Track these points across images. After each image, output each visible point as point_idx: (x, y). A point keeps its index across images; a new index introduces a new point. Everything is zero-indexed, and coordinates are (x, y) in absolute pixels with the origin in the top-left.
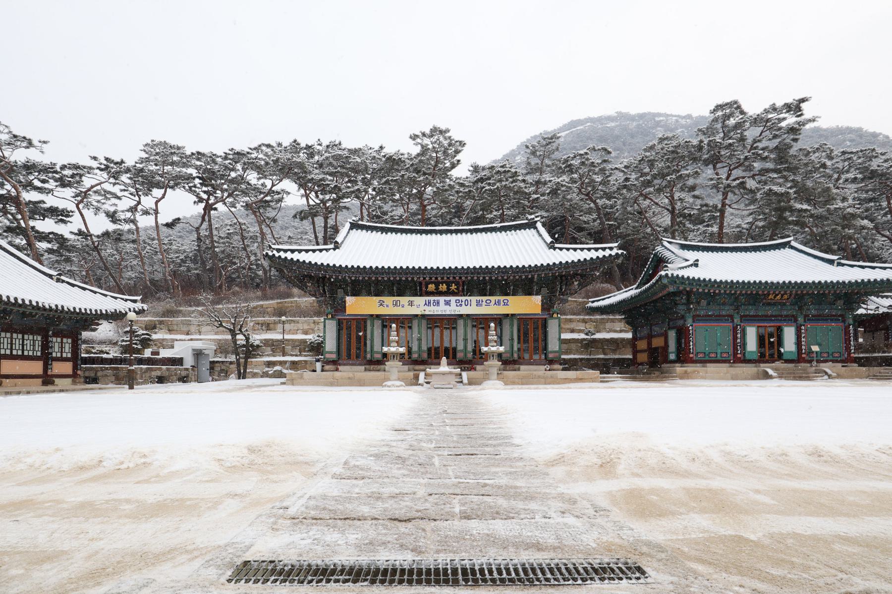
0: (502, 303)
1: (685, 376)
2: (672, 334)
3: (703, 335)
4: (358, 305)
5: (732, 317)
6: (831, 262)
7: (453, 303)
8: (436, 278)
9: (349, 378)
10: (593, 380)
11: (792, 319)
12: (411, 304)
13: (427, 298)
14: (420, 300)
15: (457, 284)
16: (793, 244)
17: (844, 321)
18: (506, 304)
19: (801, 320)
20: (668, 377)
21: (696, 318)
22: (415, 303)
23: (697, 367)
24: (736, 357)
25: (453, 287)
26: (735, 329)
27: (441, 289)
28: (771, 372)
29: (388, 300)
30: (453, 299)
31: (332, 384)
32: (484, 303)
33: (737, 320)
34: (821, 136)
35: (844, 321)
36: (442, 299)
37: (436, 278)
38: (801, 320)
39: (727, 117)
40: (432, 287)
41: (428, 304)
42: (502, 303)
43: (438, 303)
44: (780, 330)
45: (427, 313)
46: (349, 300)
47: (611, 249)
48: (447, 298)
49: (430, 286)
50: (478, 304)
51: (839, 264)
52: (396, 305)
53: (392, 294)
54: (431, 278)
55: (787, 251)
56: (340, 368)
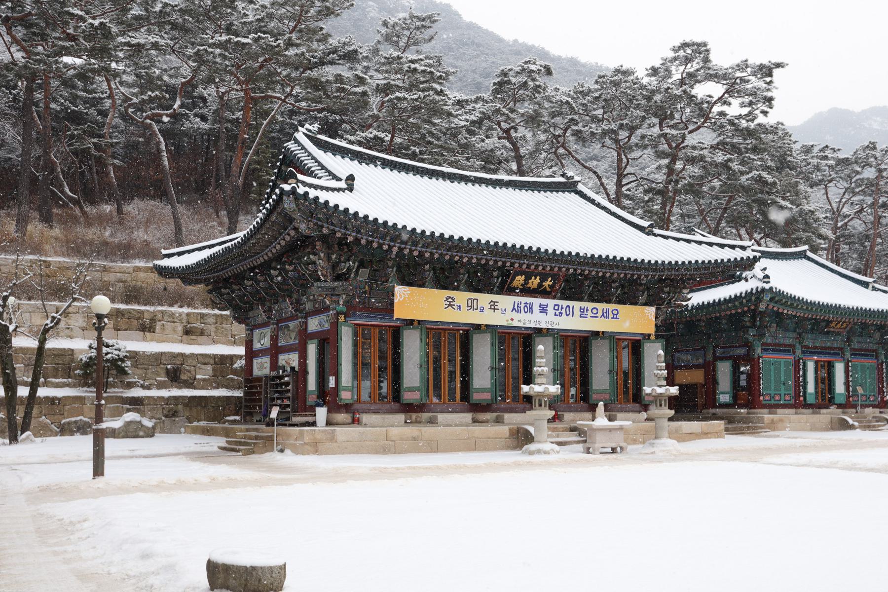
0: (611, 315)
1: (773, 426)
2: (724, 370)
3: (774, 368)
4: (415, 303)
5: (793, 346)
6: (865, 285)
7: (550, 309)
8: (544, 268)
9: (414, 439)
10: (718, 435)
11: (838, 352)
12: (493, 306)
13: (517, 299)
14: (506, 301)
15: (555, 277)
16: (809, 254)
17: (877, 358)
18: (615, 317)
19: (848, 355)
20: (754, 428)
21: (766, 348)
22: (499, 306)
23: (767, 416)
24: (799, 402)
25: (548, 283)
26: (796, 364)
27: (530, 285)
28: (851, 421)
29: (462, 297)
30: (551, 303)
31: (384, 450)
32: (590, 313)
33: (799, 352)
34: (579, 73)
35: (877, 358)
36: (536, 302)
37: (544, 268)
38: (848, 355)
39: (688, 60)
40: (520, 280)
41: (516, 309)
42: (611, 315)
43: (530, 309)
44: (830, 367)
45: (516, 324)
46: (401, 292)
47: (743, 248)
48: (544, 301)
49: (538, 280)
50: (583, 313)
51: (874, 289)
52: (471, 307)
53: (490, 291)
54: (521, 265)
55: (804, 261)
56: (365, 418)
